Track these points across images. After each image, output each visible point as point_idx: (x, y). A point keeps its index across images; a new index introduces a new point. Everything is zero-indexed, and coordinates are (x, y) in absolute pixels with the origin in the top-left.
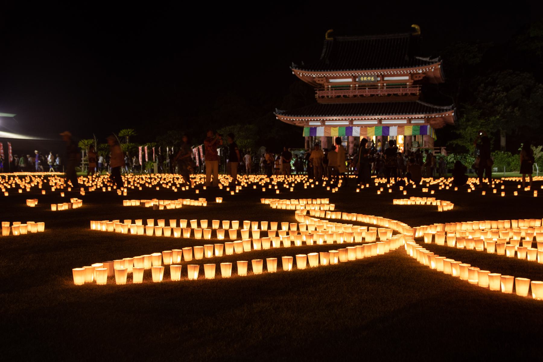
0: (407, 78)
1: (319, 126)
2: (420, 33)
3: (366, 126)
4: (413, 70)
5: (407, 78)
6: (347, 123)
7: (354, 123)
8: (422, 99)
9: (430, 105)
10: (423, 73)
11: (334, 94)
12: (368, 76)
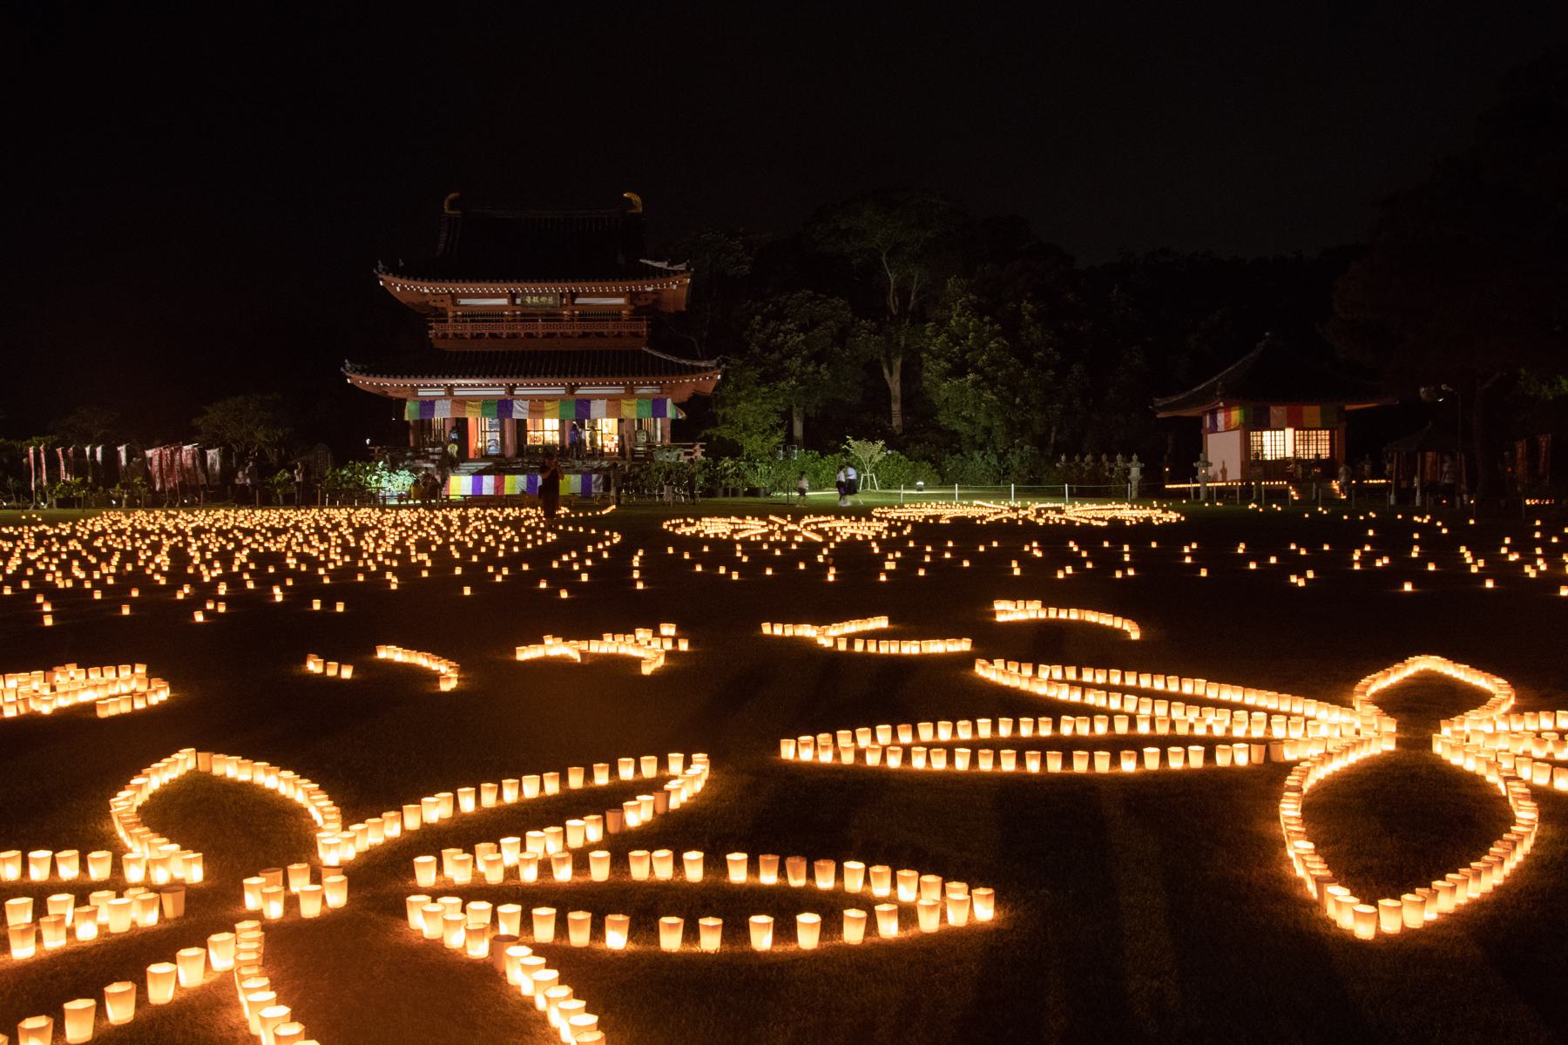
0: (621, 301)
3: (543, 399)
4: (636, 286)
5: (621, 301)
10: (653, 292)
11: (468, 329)
12: (540, 295)
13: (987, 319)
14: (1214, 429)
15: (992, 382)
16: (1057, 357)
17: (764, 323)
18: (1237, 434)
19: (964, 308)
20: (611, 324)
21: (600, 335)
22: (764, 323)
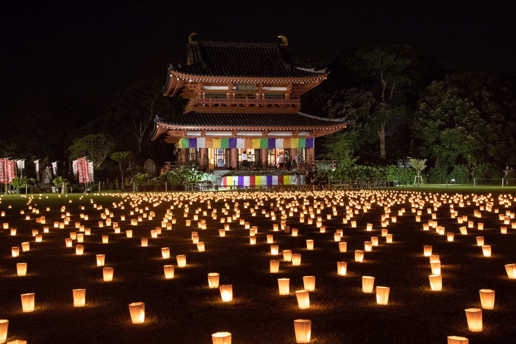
0: (284, 89)
1: (199, 137)
2: (287, 44)
3: (251, 138)
5: (284, 89)
6: (230, 134)
7: (238, 134)
8: (309, 110)
9: (316, 118)
11: (211, 102)
13: (466, 99)
15: (470, 130)
16: (503, 118)
17: (334, 103)
19: (452, 94)
21: (277, 106)
22: (334, 103)
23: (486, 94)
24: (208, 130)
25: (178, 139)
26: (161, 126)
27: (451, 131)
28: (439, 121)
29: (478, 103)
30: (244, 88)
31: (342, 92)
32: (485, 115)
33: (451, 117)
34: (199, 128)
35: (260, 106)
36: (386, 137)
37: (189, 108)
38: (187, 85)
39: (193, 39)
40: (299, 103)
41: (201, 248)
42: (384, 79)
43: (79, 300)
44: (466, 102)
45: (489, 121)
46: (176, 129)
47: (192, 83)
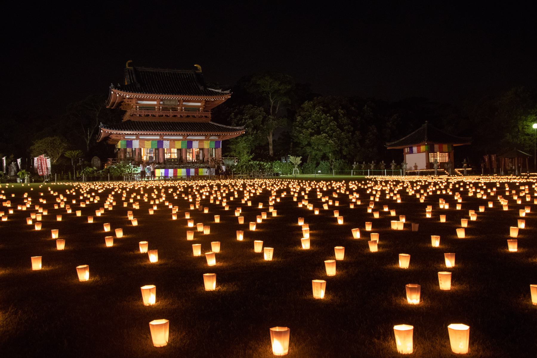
0: (199, 104)
1: (134, 139)
2: (201, 71)
5: (199, 104)
6: (158, 138)
8: (217, 120)
9: (222, 126)
11: (143, 113)
13: (328, 115)
14: (411, 152)
15: (331, 137)
17: (236, 116)
18: (424, 154)
19: (319, 111)
20: (197, 113)
21: (194, 117)
22: (236, 116)
23: (341, 111)
24: (141, 135)
25: (117, 141)
26: (104, 131)
27: (318, 137)
28: (310, 130)
29: (336, 118)
30: (168, 103)
31: (242, 107)
32: (340, 126)
33: (318, 127)
34: (135, 132)
35: (181, 116)
36: (273, 141)
37: (126, 118)
38: (124, 100)
39: (130, 65)
40: (210, 115)
41: (135, 223)
42: (272, 99)
43: (37, 265)
44: (328, 117)
45: (343, 130)
46: (117, 134)
47: (128, 98)
